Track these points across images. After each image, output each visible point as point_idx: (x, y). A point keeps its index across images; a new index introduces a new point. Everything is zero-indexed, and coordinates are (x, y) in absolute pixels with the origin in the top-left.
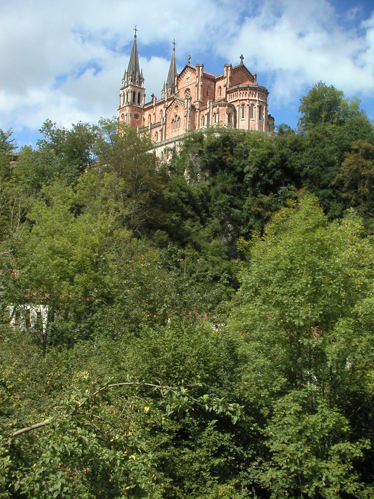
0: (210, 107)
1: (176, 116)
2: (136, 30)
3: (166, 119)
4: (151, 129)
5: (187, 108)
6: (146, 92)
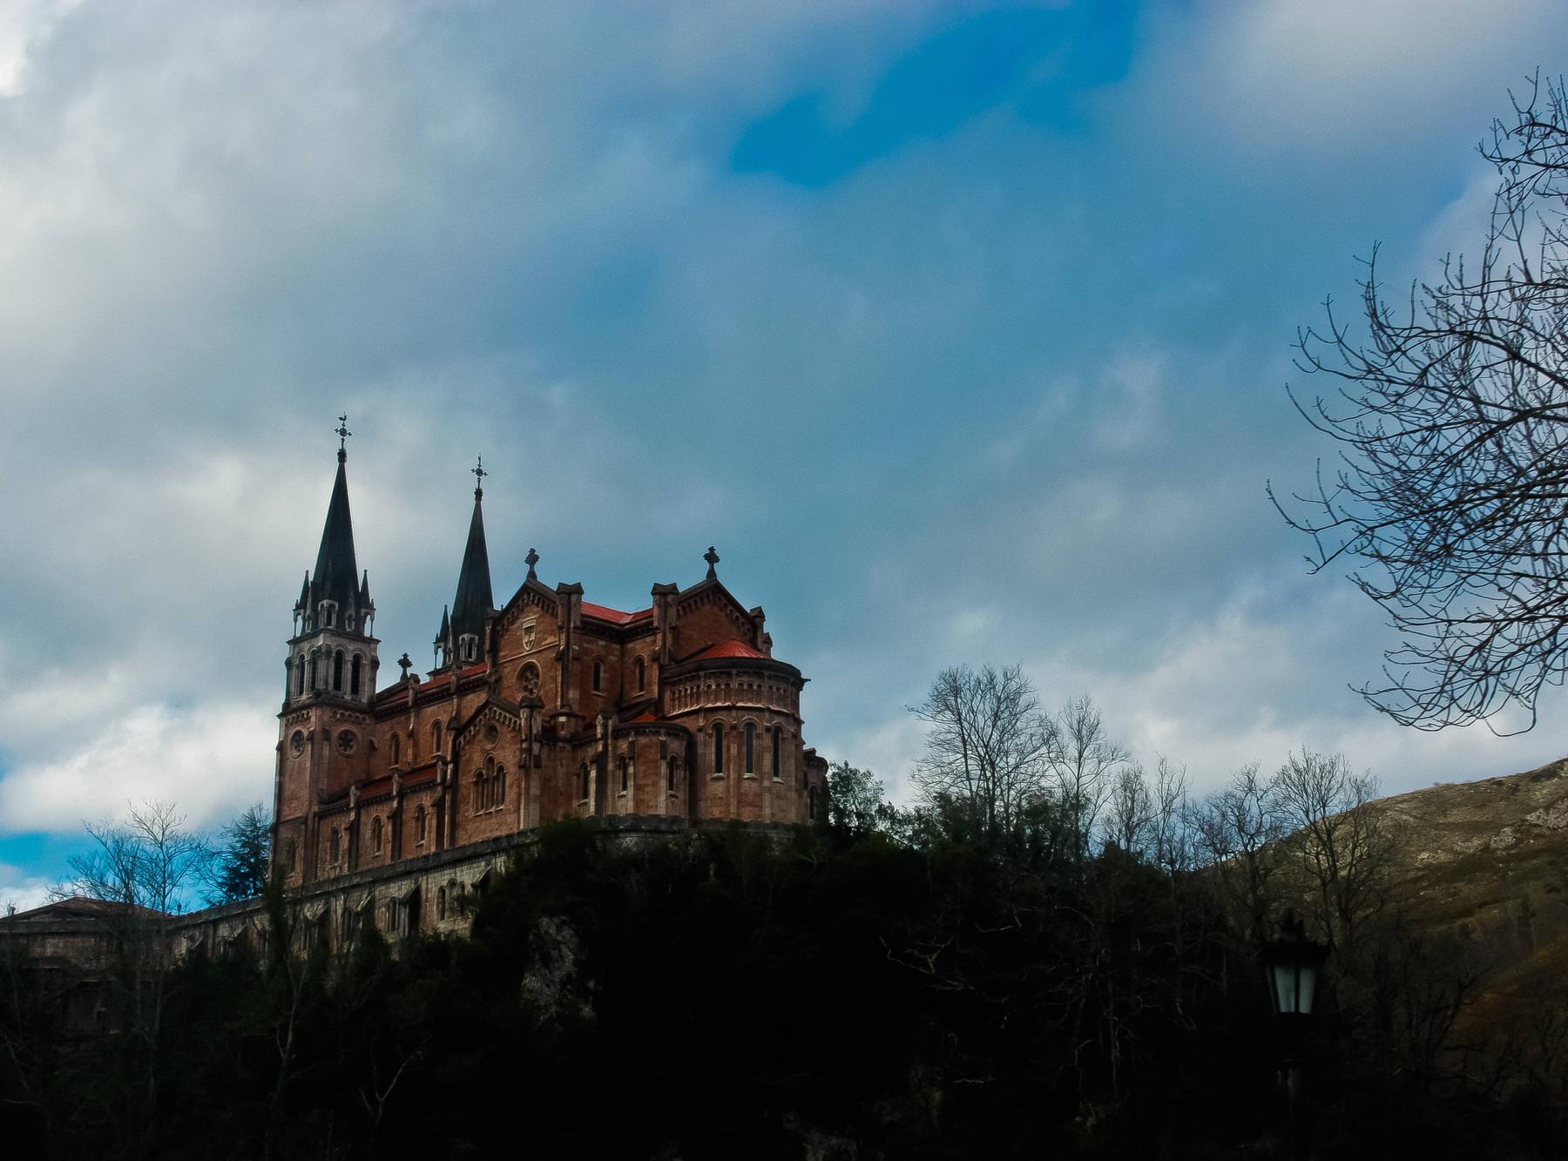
0: (605, 736)
1: (491, 760)
2: (343, 432)
3: (455, 772)
4: (402, 796)
5: (529, 739)
6: (382, 653)
